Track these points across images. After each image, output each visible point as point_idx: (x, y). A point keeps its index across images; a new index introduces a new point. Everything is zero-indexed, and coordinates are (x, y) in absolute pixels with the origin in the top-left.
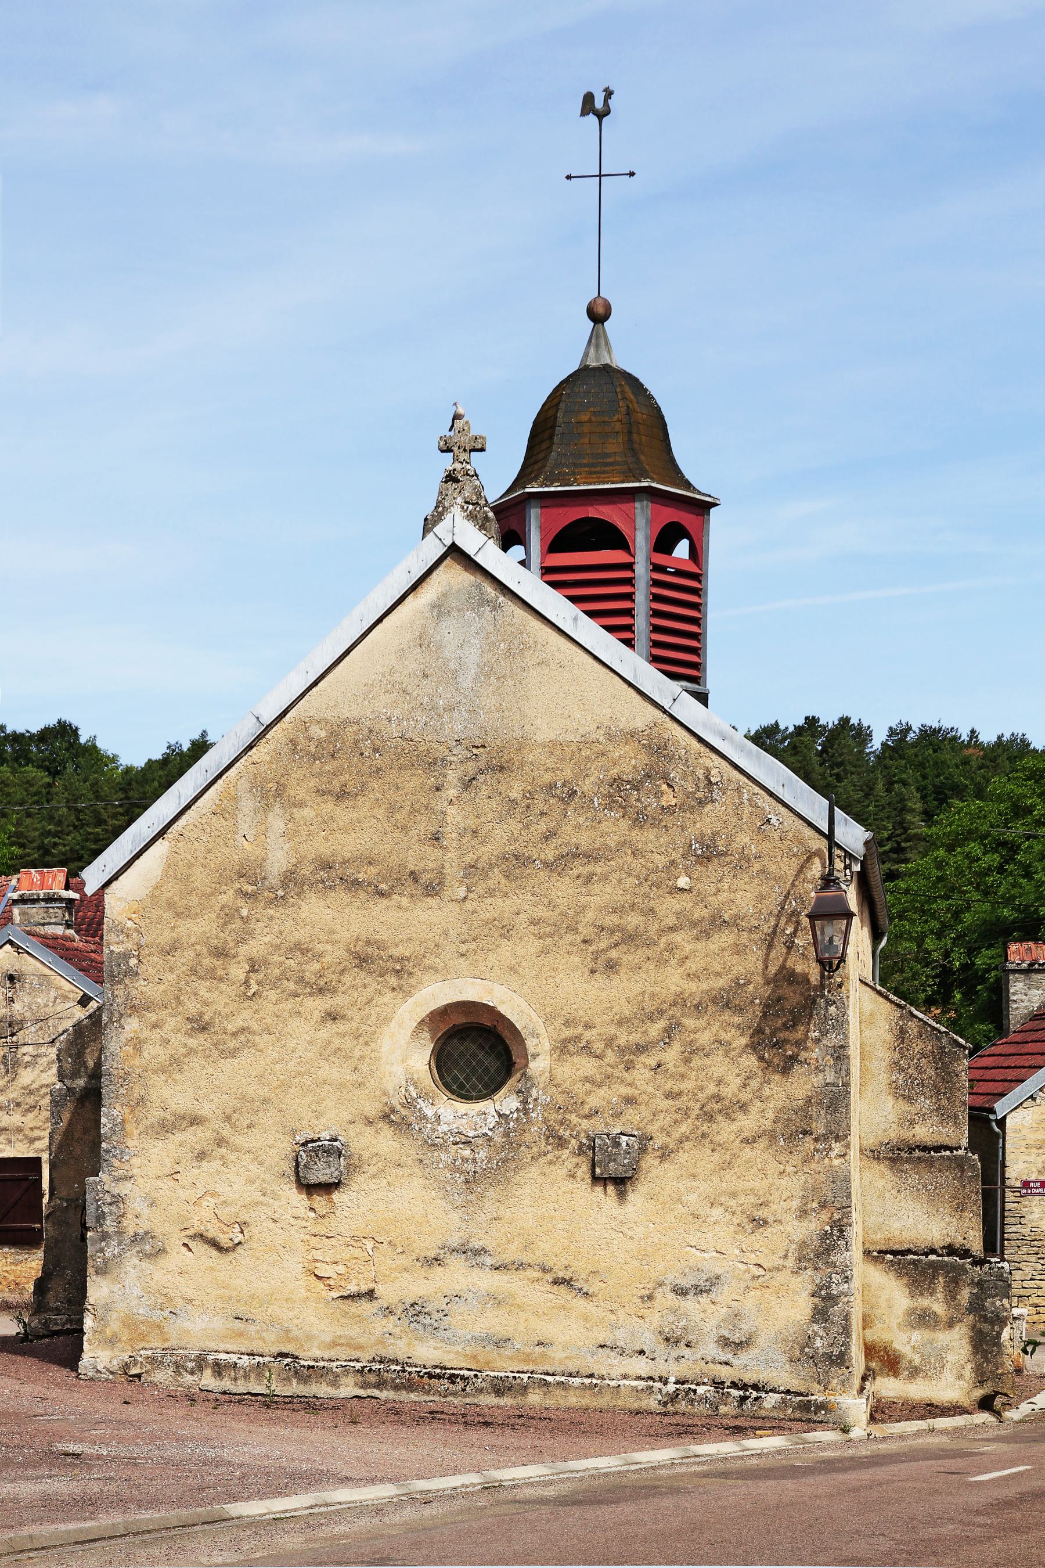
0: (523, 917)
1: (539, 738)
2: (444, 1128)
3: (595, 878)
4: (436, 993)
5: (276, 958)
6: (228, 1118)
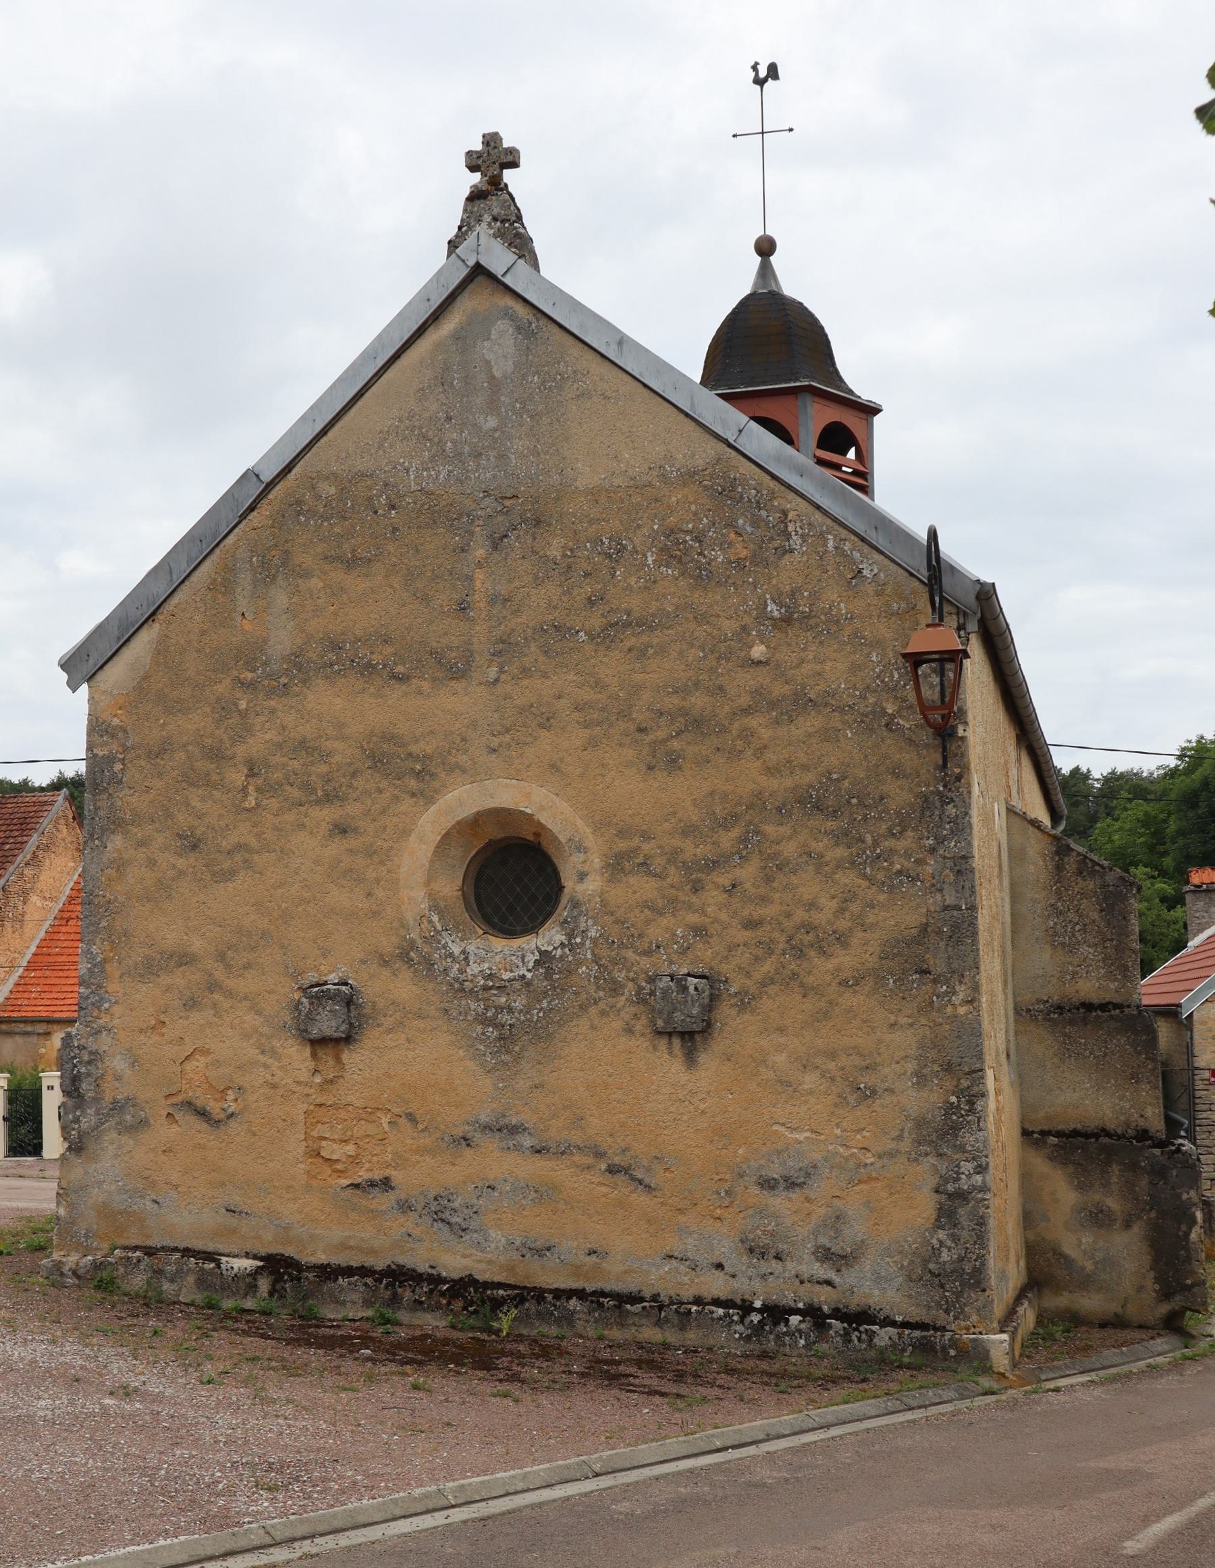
0: (564, 702)
1: (581, 484)
2: (474, 969)
3: (651, 651)
4: (462, 799)
5: (278, 759)
6: (221, 957)
